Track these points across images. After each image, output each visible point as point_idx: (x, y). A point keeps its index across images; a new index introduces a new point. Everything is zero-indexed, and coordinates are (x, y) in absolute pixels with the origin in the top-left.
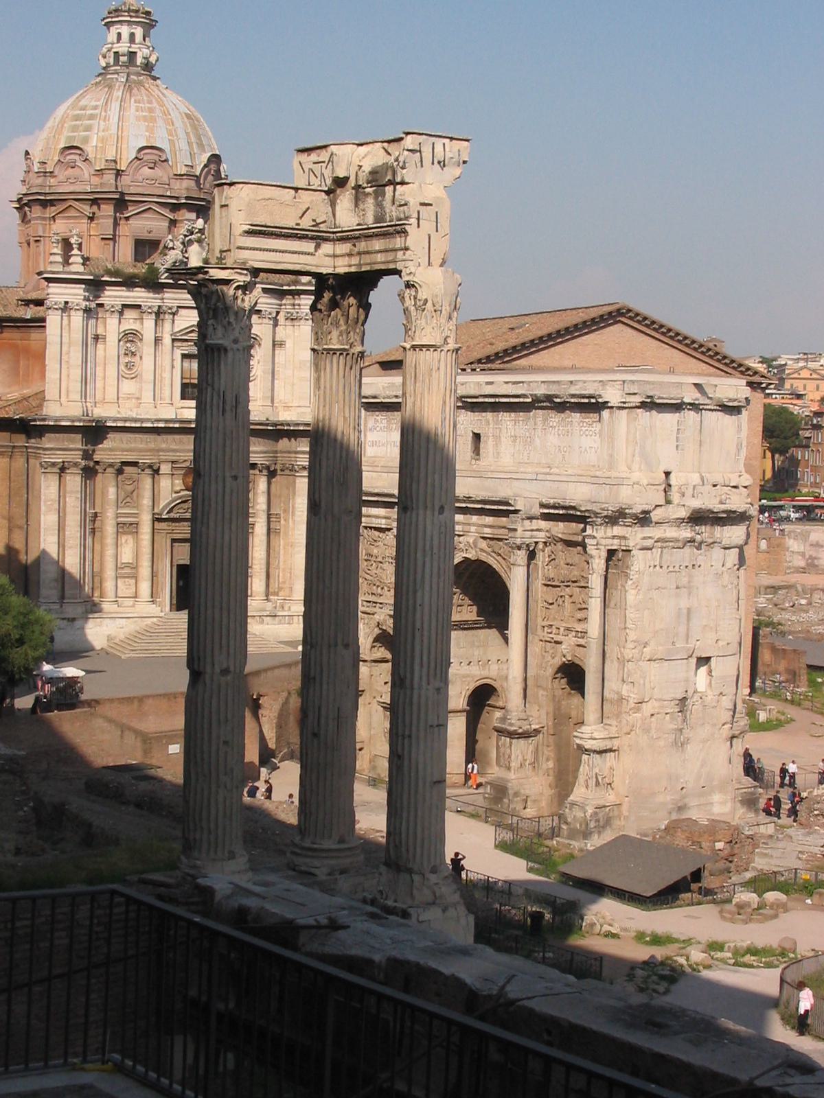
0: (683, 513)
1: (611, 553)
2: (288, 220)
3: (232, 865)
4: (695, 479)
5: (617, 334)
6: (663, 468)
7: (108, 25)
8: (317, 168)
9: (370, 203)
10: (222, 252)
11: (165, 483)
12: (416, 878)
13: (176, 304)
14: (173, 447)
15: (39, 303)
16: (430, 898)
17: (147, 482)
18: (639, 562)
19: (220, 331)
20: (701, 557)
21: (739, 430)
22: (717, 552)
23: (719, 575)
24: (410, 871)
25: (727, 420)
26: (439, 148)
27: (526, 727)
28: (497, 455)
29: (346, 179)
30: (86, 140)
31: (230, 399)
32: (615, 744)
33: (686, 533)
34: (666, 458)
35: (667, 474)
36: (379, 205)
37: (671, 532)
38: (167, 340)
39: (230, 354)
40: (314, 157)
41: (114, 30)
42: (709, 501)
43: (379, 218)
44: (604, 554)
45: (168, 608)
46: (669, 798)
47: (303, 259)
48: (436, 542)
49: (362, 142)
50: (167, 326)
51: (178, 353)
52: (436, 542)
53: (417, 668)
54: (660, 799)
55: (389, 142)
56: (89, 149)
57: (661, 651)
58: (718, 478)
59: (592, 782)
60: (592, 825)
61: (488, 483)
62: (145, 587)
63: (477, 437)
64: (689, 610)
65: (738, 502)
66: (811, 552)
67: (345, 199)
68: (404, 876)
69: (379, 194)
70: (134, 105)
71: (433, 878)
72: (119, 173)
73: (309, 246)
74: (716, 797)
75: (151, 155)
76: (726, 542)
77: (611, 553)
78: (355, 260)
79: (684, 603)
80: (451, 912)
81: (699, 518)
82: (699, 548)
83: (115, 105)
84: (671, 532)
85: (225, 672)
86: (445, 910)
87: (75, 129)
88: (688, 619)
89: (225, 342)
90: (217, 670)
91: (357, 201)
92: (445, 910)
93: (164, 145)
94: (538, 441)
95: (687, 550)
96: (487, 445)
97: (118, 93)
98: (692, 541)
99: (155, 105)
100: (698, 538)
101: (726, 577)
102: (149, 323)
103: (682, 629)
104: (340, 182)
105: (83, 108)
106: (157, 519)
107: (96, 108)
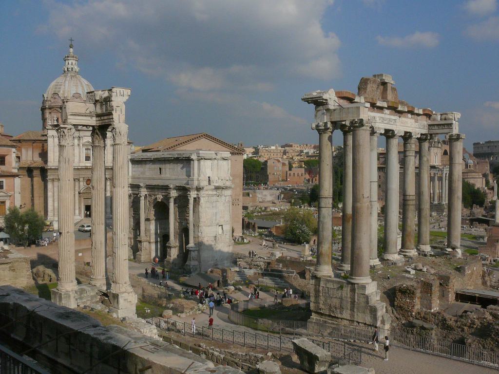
1: (195, 198)
2: (83, 111)
3: (71, 284)
5: (204, 142)
6: (208, 176)
7: (65, 60)
8: (91, 97)
9: (104, 107)
11: (81, 183)
12: (121, 285)
13: (83, 135)
14: (83, 173)
15: (46, 135)
16: (125, 291)
17: (77, 183)
18: (202, 200)
19: (64, 141)
22: (223, 198)
23: (224, 204)
24: (119, 283)
25: (225, 162)
26: (122, 92)
27: (175, 245)
28: (166, 173)
29: (99, 100)
30: (59, 91)
31: (67, 160)
34: (209, 173)
35: (209, 177)
36: (106, 107)
37: (210, 193)
38: (81, 145)
39: (67, 147)
41: (67, 62)
42: (220, 184)
43: (106, 110)
44: (193, 199)
45: (83, 217)
46: (212, 262)
47: (87, 122)
48: (122, 196)
50: (81, 141)
51: (84, 148)
52: (122, 196)
53: (118, 229)
54: (210, 263)
56: (60, 95)
59: (192, 259)
60: (192, 270)
61: (163, 181)
62: (77, 212)
63: (160, 169)
64: (216, 213)
65: (228, 184)
66: (264, 197)
67: (98, 106)
68: (118, 285)
69: (107, 104)
70: (72, 82)
71: (125, 285)
73: (89, 118)
74: (226, 262)
76: (226, 195)
77: (195, 198)
78: (101, 122)
80: (130, 294)
81: (217, 188)
82: (218, 196)
83: (67, 82)
84: (210, 193)
85: (68, 232)
86: (129, 294)
87: (56, 88)
88: (216, 215)
89: (66, 145)
90: (66, 232)
91: (101, 106)
92: (129, 294)
93: (81, 93)
94: (176, 170)
96: (163, 171)
97: (68, 79)
98: (216, 194)
99: (78, 82)
100: (218, 194)
101: (226, 204)
102: (76, 141)
103: (214, 218)
104: (96, 101)
105: (58, 83)
106: (79, 193)
107: (61, 83)
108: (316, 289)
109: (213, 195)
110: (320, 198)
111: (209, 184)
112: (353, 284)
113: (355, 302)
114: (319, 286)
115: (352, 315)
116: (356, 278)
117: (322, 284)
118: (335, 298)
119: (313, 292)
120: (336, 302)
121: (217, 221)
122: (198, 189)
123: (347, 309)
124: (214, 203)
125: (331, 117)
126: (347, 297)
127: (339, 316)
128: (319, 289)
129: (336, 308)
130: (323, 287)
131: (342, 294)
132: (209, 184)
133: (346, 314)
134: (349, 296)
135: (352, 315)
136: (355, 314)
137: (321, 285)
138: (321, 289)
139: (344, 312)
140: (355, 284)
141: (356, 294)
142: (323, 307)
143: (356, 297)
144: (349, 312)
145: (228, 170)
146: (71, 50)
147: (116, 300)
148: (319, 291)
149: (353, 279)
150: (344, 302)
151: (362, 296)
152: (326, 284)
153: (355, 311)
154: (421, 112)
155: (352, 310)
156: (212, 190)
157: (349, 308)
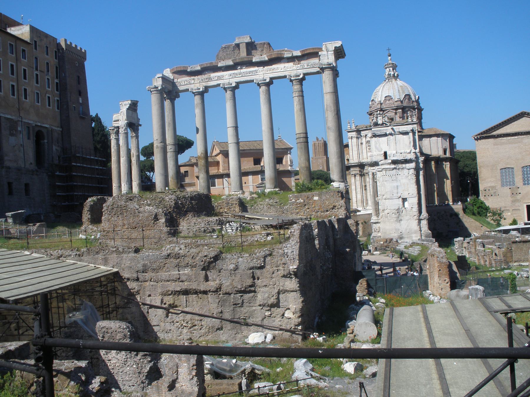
0: (390, 161)
4: (394, 152)
7: (386, 68)
20: (400, 172)
21: (409, 138)
22: (406, 171)
32: (379, 221)
33: (393, 166)
37: (388, 166)
41: (388, 69)
46: (396, 235)
57: (388, 197)
58: (402, 151)
64: (397, 186)
72: (381, 104)
75: (388, 98)
79: (395, 184)
84: (388, 166)
95: (394, 171)
101: (410, 177)
103: (395, 191)
109: (393, 169)
111: (386, 157)
121: (399, 195)
122: (375, 164)
124: (394, 176)
132: (386, 157)
145: (410, 143)
146: (389, 58)
154: (298, 53)
156: (390, 164)
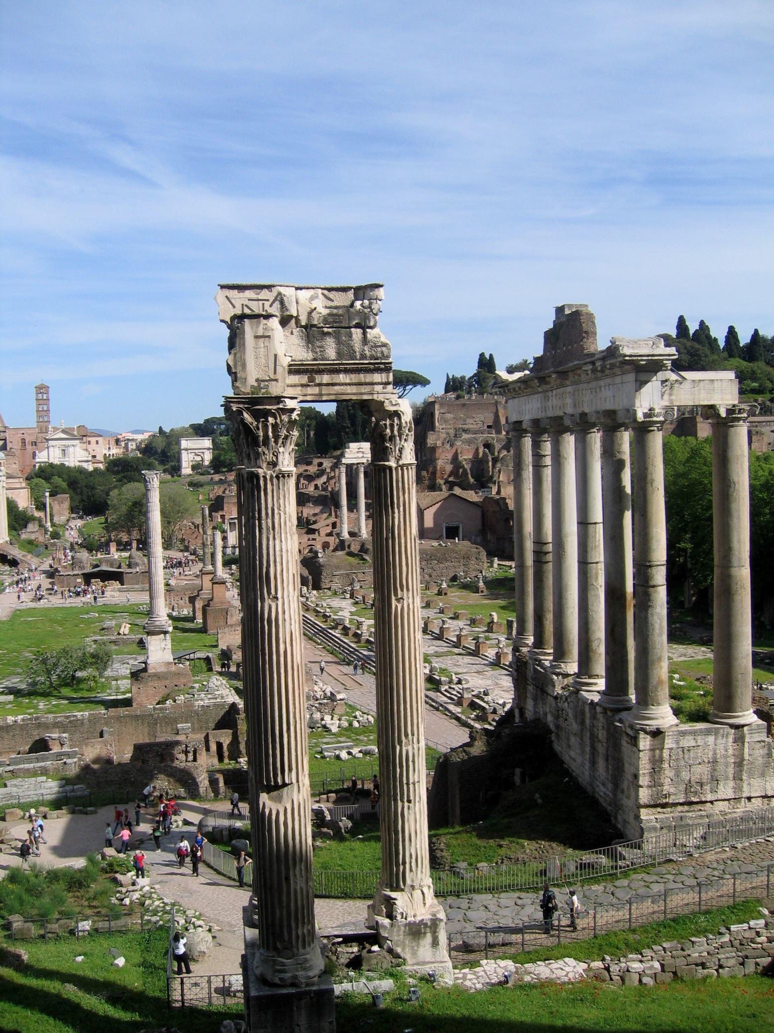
10: (257, 380)
40: (249, 294)
49: (300, 285)
55: (330, 290)
108: (654, 756)
110: (650, 566)
112: (738, 727)
113: (743, 759)
114: (662, 749)
115: (738, 789)
116: (746, 713)
117: (669, 743)
118: (700, 764)
119: (648, 766)
120: (701, 771)
123: (727, 778)
125: (673, 397)
126: (726, 757)
127: (709, 797)
128: (661, 756)
129: (702, 784)
130: (671, 749)
131: (715, 754)
133: (726, 790)
134: (730, 752)
135: (738, 789)
136: (745, 785)
137: (666, 746)
138: (666, 754)
139: (721, 787)
140: (743, 726)
141: (746, 745)
142: (672, 790)
143: (746, 750)
144: (731, 784)
147: (429, 938)
148: (661, 760)
149: (739, 717)
150: (720, 768)
151: (758, 745)
152: (677, 742)
153: (744, 778)
155: (738, 778)
157: (731, 776)
